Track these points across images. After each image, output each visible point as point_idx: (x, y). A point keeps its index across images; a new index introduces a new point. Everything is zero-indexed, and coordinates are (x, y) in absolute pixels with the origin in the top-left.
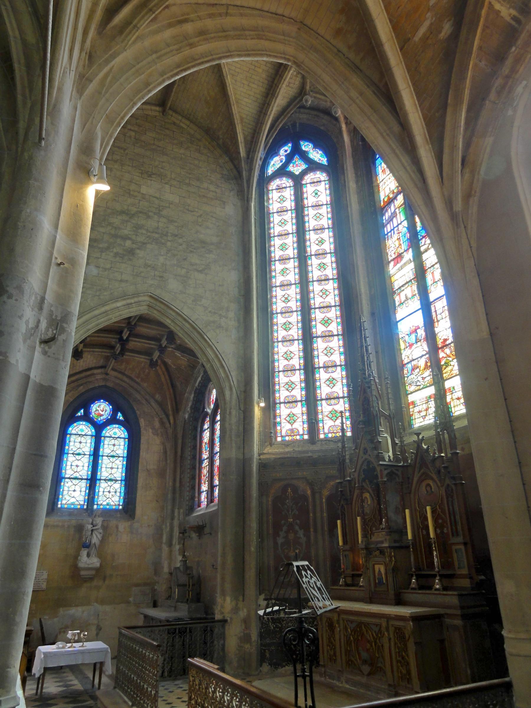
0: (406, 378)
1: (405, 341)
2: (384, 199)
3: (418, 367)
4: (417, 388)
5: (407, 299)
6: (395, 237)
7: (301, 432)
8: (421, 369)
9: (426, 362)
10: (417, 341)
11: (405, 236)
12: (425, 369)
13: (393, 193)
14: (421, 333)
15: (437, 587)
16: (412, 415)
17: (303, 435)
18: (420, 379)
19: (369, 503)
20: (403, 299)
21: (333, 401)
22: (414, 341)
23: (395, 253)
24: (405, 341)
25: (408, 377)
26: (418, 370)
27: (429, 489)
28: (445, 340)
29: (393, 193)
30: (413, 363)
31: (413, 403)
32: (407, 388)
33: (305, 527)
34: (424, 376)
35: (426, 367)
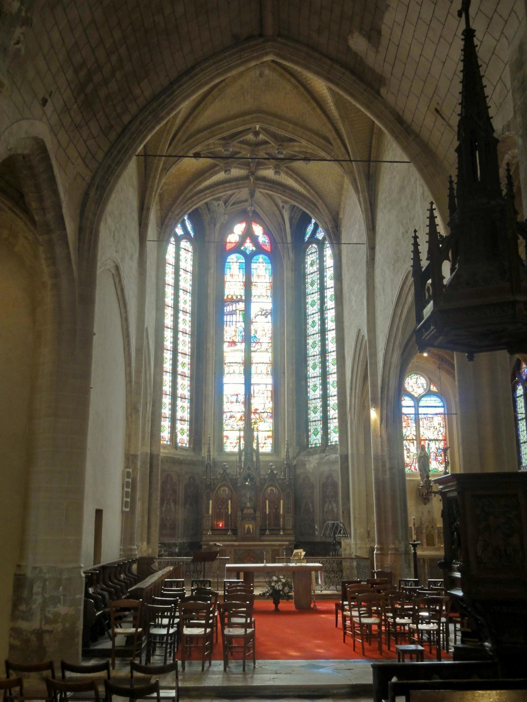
0: (224, 421)
1: (228, 398)
2: (228, 296)
3: (234, 417)
4: (232, 429)
5: (234, 373)
6: (233, 328)
7: (167, 440)
8: (237, 419)
9: (241, 417)
10: (237, 401)
11: (241, 333)
12: (240, 420)
13: (237, 297)
14: (242, 398)
15: (281, 533)
16: (225, 443)
17: (167, 441)
18: (235, 424)
19: (227, 492)
20: (231, 371)
21: (183, 422)
22: (235, 401)
23: (230, 338)
24: (228, 398)
25: (226, 420)
26: (234, 419)
27: (272, 491)
28: (256, 410)
29: (237, 297)
30: (231, 413)
31: (227, 437)
32: (224, 426)
33: (175, 502)
34: (238, 424)
35: (241, 419)
